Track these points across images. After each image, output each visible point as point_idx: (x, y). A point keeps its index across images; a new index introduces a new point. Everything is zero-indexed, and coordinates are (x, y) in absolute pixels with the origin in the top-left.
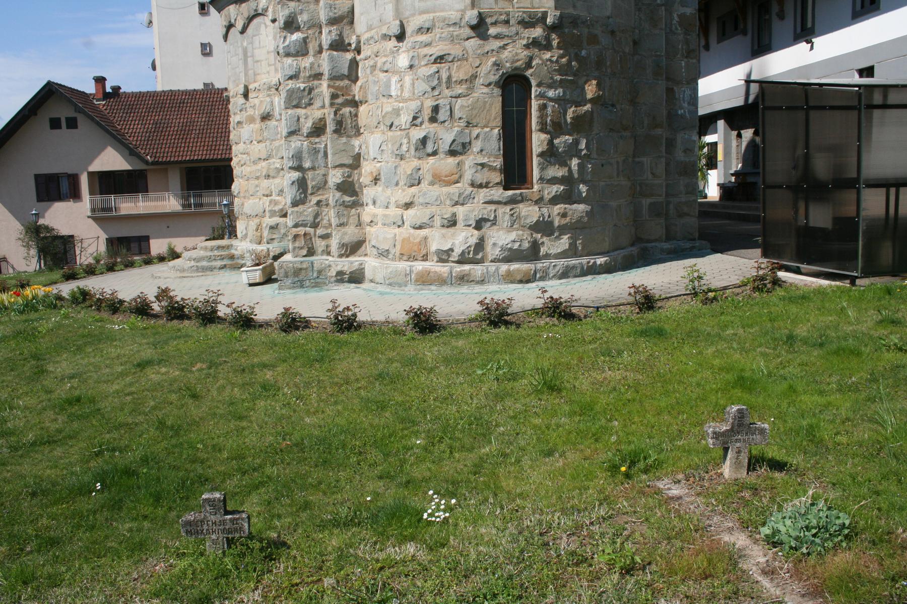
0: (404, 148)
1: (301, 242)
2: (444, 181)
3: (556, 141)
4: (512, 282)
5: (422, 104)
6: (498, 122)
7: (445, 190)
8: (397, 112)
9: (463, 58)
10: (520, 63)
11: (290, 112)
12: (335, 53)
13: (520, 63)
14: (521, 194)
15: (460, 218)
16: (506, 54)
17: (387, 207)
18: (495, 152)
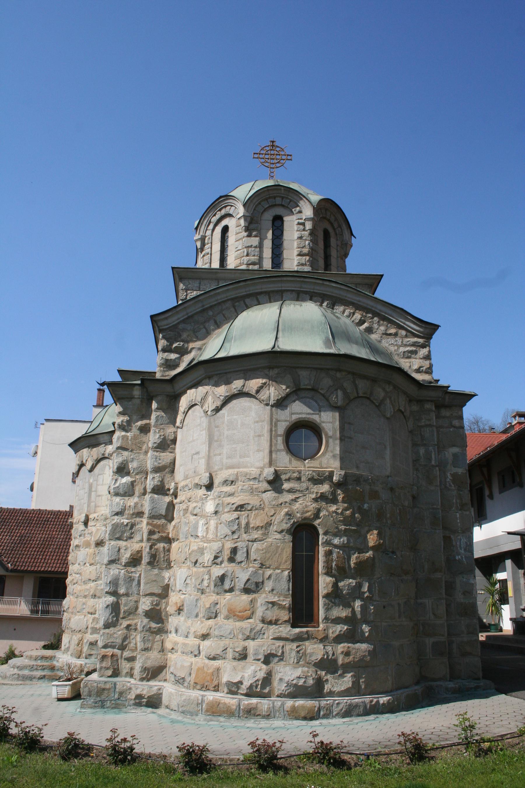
0: (205, 583)
1: (107, 663)
2: (238, 616)
3: (341, 584)
4: (297, 718)
5: (223, 546)
6: (289, 565)
7: (239, 624)
8: (201, 551)
9: (261, 508)
11: (113, 543)
12: (156, 496)
15: (251, 652)
16: (297, 506)
17: (187, 637)
18: (285, 592)
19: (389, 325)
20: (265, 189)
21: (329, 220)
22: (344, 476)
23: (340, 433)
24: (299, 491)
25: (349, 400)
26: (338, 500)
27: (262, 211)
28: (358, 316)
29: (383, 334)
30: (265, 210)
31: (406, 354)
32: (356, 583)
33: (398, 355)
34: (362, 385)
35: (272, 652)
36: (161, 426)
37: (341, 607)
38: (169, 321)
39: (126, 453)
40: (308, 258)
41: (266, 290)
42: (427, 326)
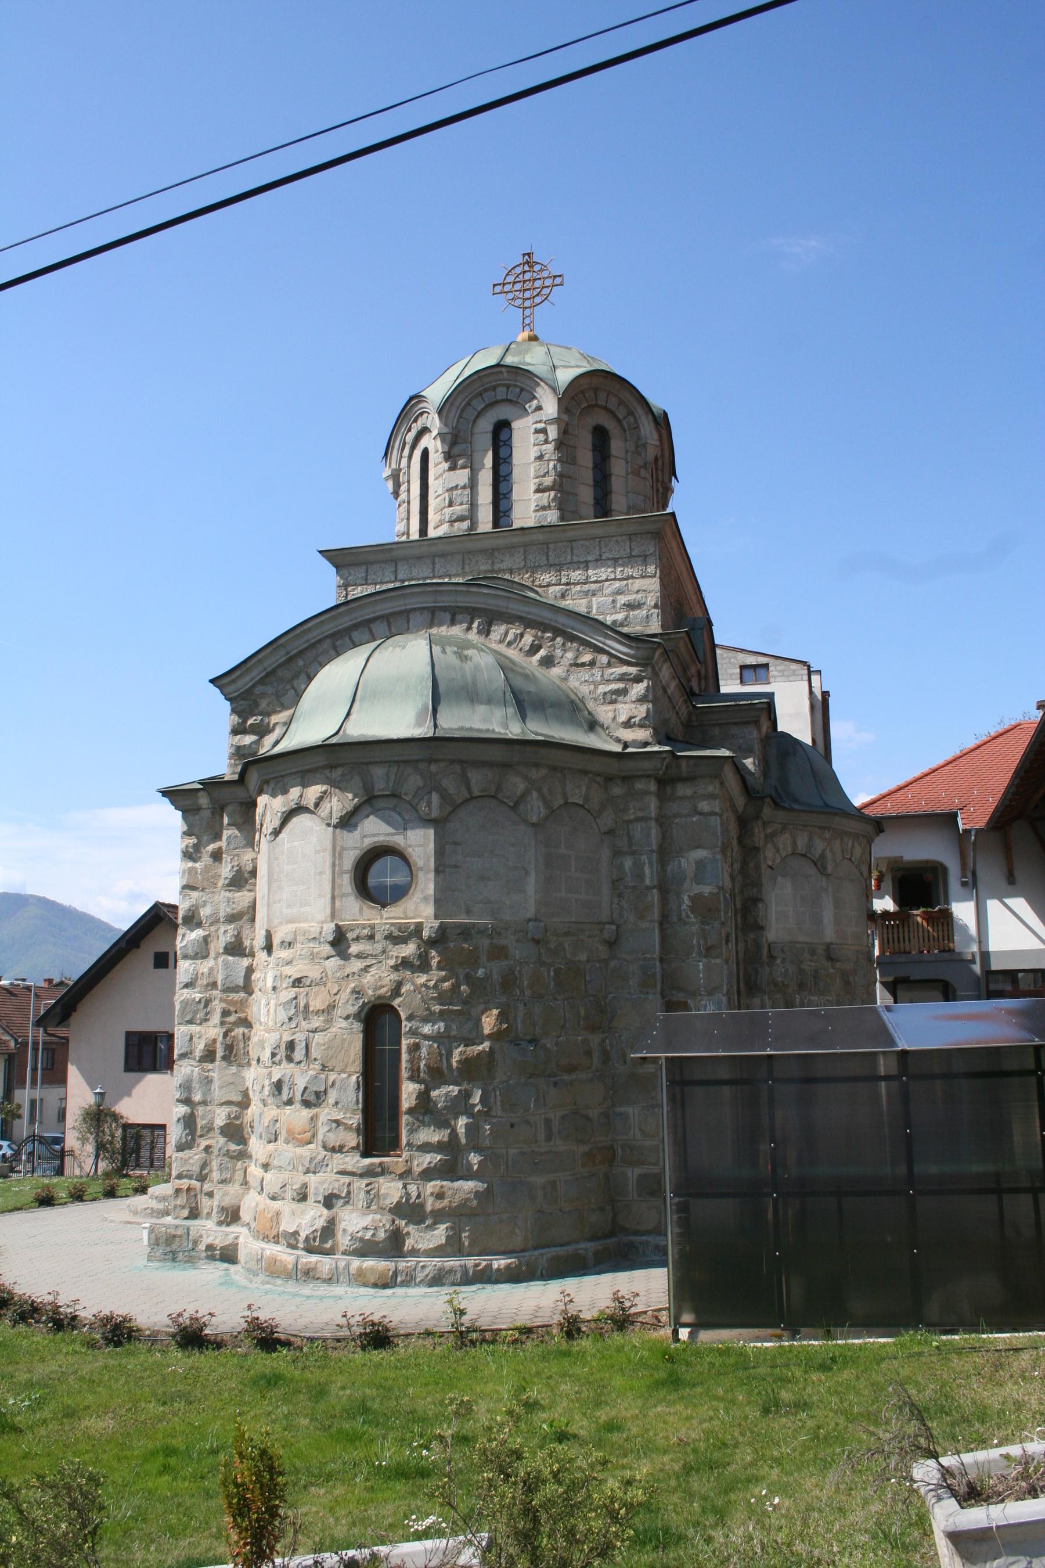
1: (181, 1200)
2: (297, 1139)
3: (434, 1094)
4: (365, 1285)
5: (281, 1038)
6: (357, 1066)
7: (300, 1150)
9: (321, 982)
10: (385, 989)
12: (231, 958)
13: (385, 989)
14: (381, 1164)
15: (311, 1190)
16: (368, 979)
19: (581, 648)
20: (475, 377)
21: (605, 408)
22: (438, 930)
24: (372, 955)
25: (453, 807)
26: (431, 966)
27: (472, 418)
28: (528, 639)
29: (571, 665)
30: (479, 415)
31: (609, 696)
32: (460, 1091)
33: (595, 699)
34: (477, 778)
38: (240, 684)
39: (195, 894)
40: (552, 493)
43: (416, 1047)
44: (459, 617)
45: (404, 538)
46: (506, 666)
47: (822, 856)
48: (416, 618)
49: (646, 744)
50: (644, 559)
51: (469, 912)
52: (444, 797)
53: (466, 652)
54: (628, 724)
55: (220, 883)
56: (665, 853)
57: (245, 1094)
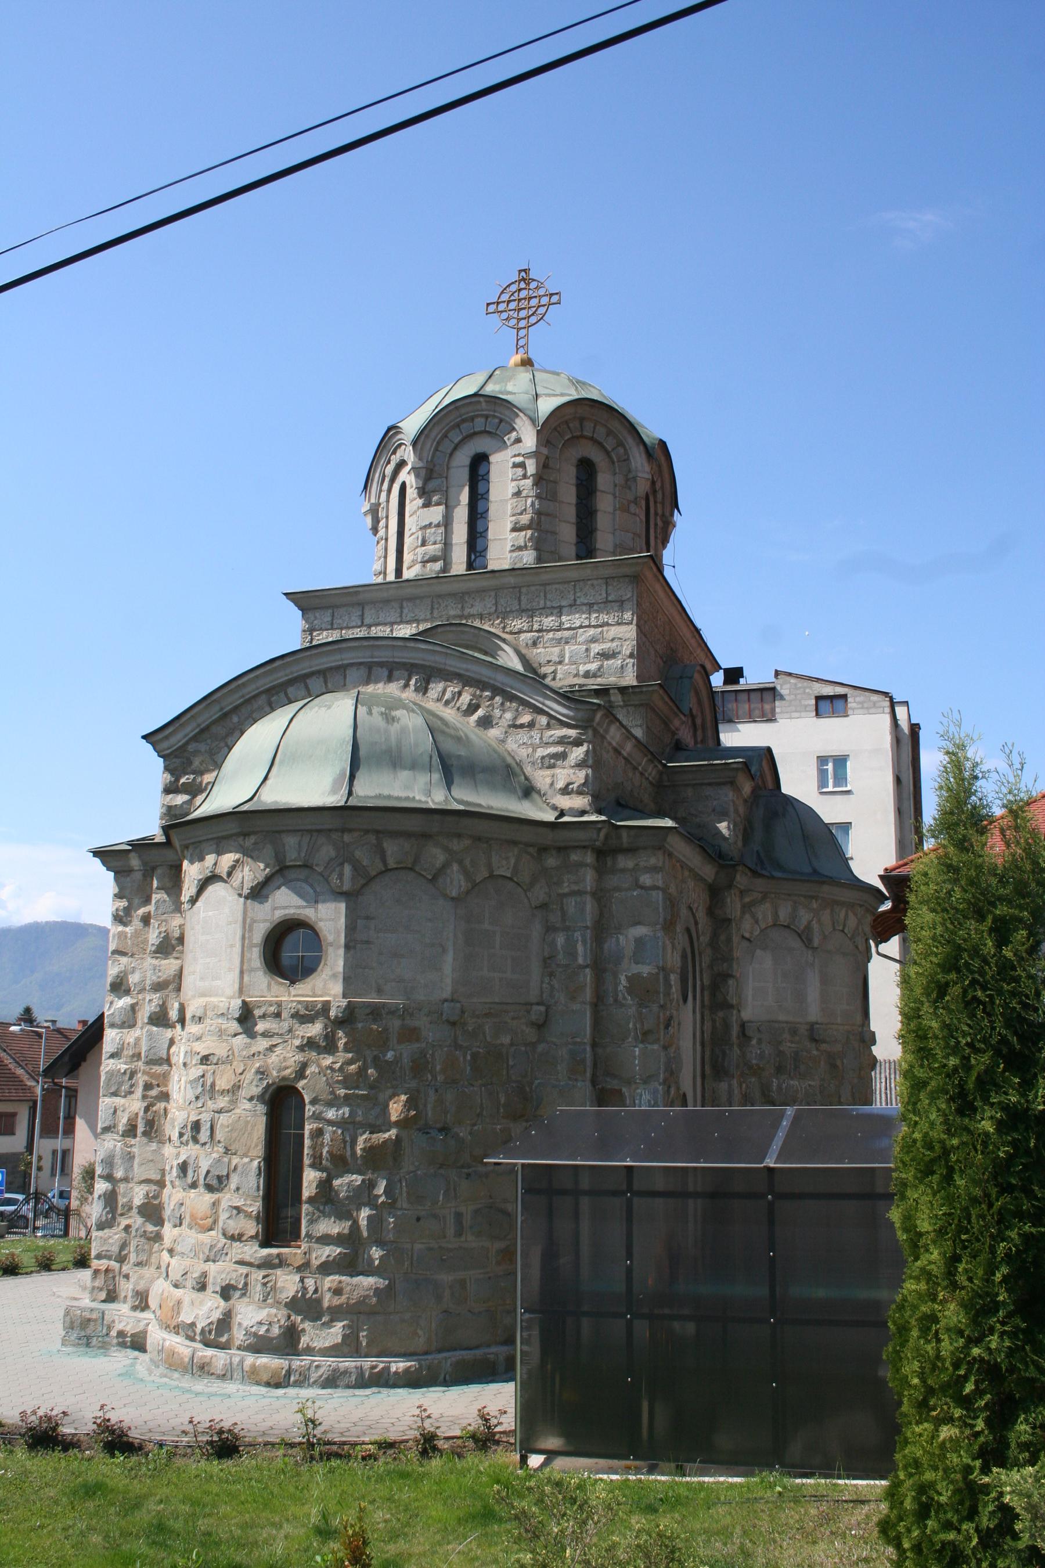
3: (336, 1183)
4: (258, 1383)
6: (258, 1150)
9: (228, 1061)
10: (288, 1071)
12: (155, 1029)
13: (288, 1071)
14: (278, 1255)
15: (210, 1280)
16: (273, 1059)
19: (521, 708)
20: (452, 407)
21: (592, 439)
22: (345, 1009)
23: (346, 937)
24: (277, 1034)
25: (365, 880)
26: (337, 1048)
27: (449, 451)
28: (466, 698)
29: (510, 726)
30: (455, 448)
31: (547, 760)
32: (363, 1181)
33: (533, 763)
34: (392, 849)
35: (232, 1282)
36: (164, 917)
37: (333, 1219)
38: (173, 740)
39: (124, 960)
40: (529, 532)
41: (318, 668)
42: (579, 706)
43: (318, 1133)
44: (396, 673)
45: (380, 579)
46: (435, 728)
47: (808, 927)
48: (352, 674)
49: (583, 813)
50: (621, 604)
51: (380, 991)
52: (357, 867)
53: (394, 713)
54: (565, 791)
55: (150, 948)
56: (601, 930)
57: (163, 1172)
